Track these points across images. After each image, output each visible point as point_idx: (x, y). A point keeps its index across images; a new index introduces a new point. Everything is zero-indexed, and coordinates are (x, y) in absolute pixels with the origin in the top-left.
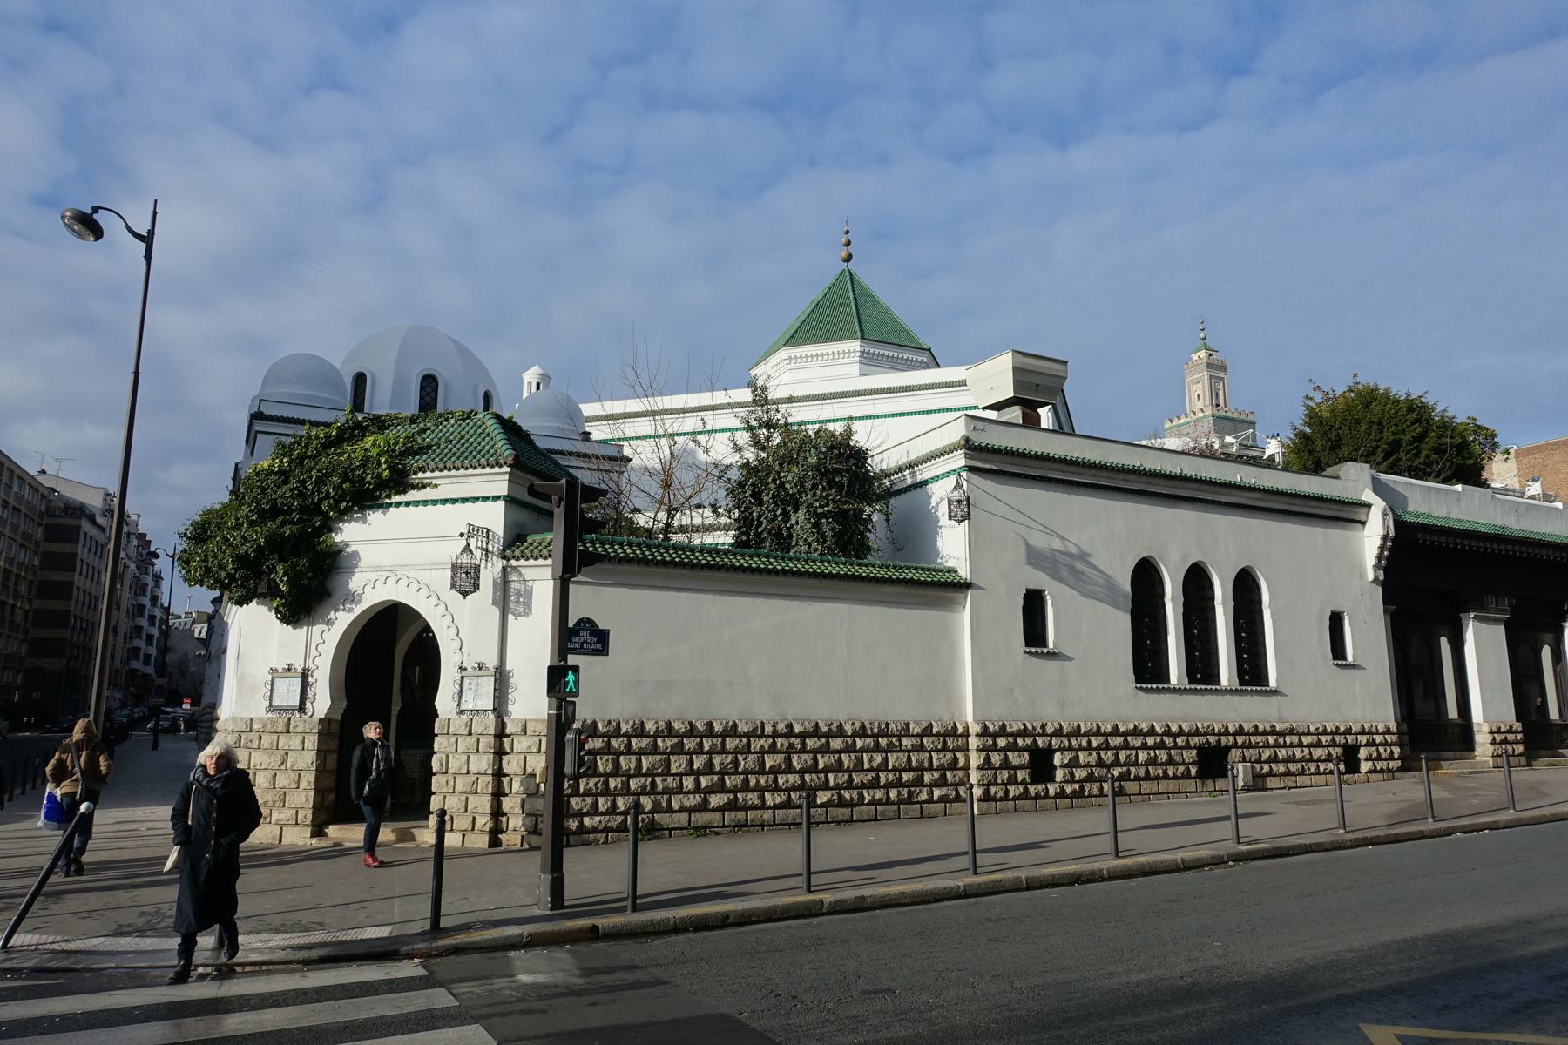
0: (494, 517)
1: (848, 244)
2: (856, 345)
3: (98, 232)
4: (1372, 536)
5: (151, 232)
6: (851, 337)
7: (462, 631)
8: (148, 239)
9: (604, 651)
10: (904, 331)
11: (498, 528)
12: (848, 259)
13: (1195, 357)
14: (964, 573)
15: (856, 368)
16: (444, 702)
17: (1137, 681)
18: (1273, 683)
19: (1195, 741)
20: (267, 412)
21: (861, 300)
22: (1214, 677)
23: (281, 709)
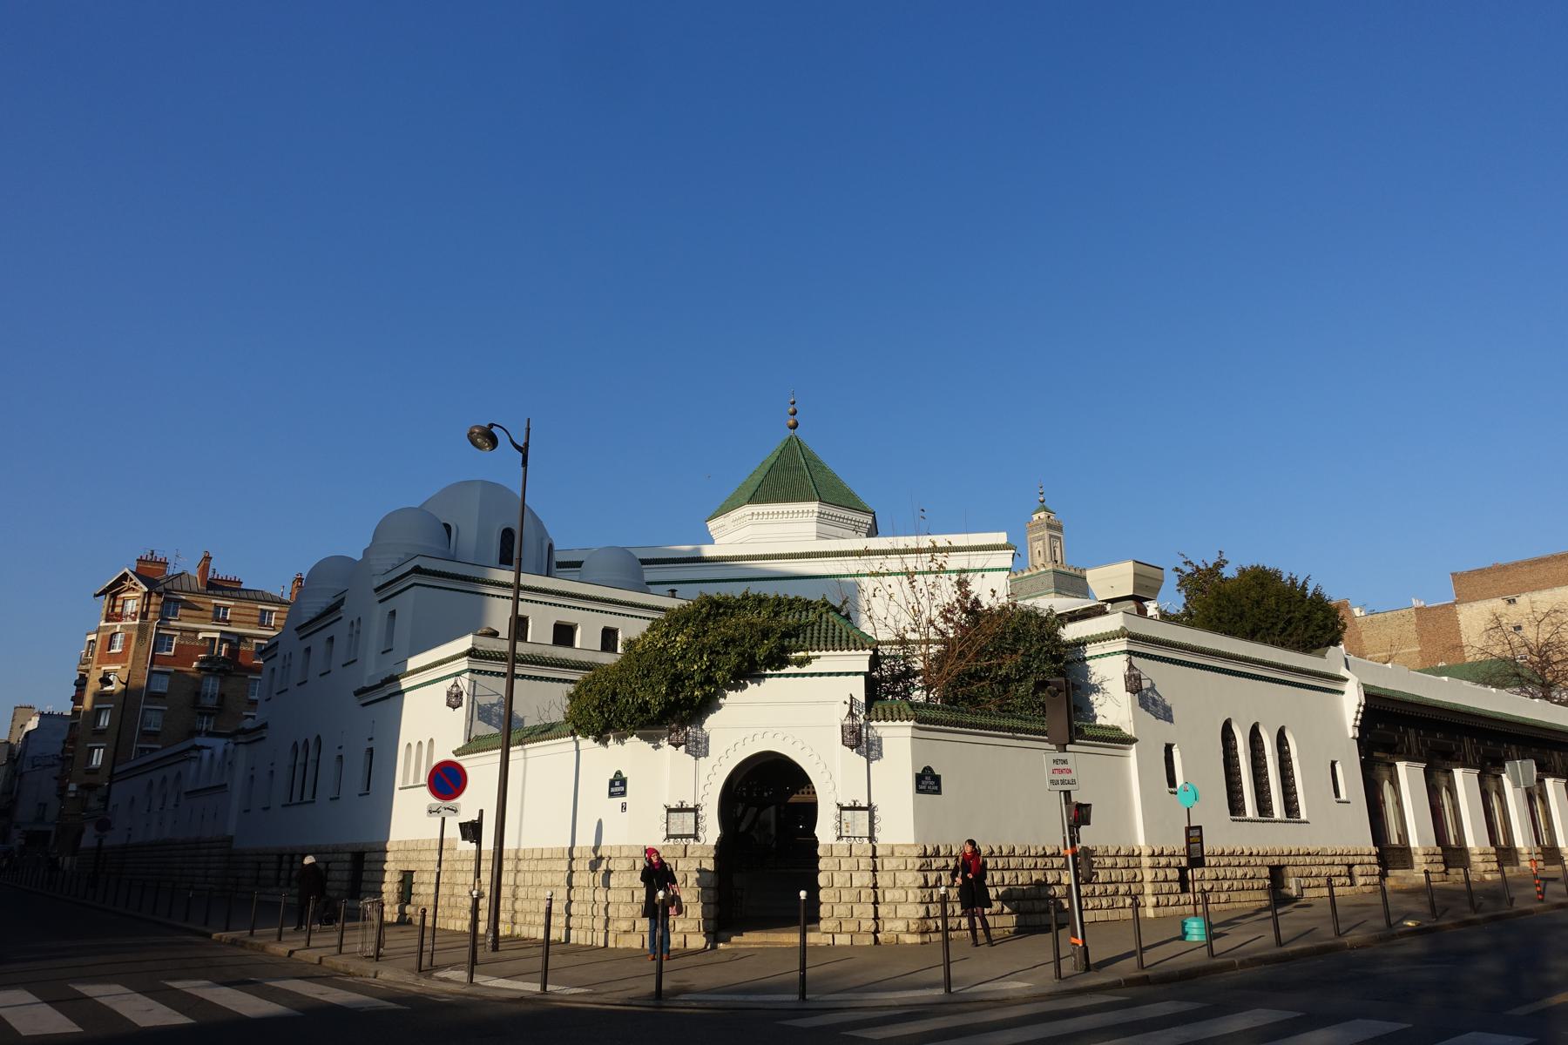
0: (858, 688)
1: (794, 413)
2: (814, 506)
3: (493, 442)
4: (1350, 704)
5: (527, 445)
6: (812, 500)
7: (834, 778)
8: (524, 450)
9: (938, 792)
10: (858, 502)
11: (861, 697)
12: (795, 426)
13: (1035, 517)
14: (1128, 730)
15: (812, 528)
16: (825, 831)
17: (1232, 814)
18: (1303, 816)
19: (1268, 861)
21: (811, 464)
22: (1242, 810)
23: (675, 837)
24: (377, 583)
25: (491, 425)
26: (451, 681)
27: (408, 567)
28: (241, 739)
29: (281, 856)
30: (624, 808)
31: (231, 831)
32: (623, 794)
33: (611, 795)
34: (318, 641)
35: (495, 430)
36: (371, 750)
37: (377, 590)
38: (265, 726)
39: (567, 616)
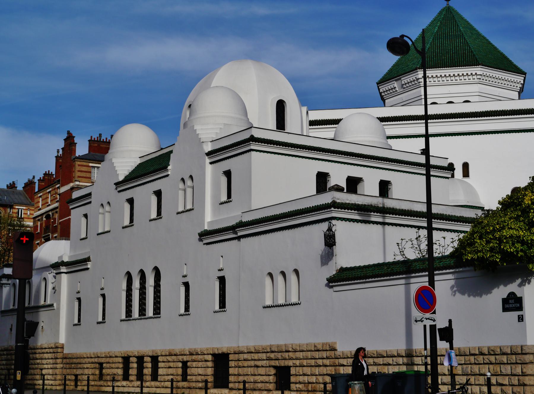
20: (256, 136)
24: (209, 148)
25: (402, 36)
26: (324, 226)
27: (246, 136)
28: (63, 269)
29: (126, 360)
30: (521, 319)
31: (62, 340)
32: (520, 308)
33: (505, 310)
34: (144, 194)
35: (405, 38)
36: (222, 280)
37: (209, 154)
38: (88, 260)
39: (356, 172)
